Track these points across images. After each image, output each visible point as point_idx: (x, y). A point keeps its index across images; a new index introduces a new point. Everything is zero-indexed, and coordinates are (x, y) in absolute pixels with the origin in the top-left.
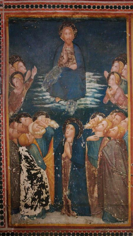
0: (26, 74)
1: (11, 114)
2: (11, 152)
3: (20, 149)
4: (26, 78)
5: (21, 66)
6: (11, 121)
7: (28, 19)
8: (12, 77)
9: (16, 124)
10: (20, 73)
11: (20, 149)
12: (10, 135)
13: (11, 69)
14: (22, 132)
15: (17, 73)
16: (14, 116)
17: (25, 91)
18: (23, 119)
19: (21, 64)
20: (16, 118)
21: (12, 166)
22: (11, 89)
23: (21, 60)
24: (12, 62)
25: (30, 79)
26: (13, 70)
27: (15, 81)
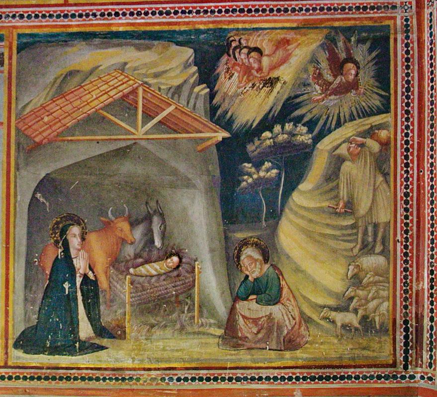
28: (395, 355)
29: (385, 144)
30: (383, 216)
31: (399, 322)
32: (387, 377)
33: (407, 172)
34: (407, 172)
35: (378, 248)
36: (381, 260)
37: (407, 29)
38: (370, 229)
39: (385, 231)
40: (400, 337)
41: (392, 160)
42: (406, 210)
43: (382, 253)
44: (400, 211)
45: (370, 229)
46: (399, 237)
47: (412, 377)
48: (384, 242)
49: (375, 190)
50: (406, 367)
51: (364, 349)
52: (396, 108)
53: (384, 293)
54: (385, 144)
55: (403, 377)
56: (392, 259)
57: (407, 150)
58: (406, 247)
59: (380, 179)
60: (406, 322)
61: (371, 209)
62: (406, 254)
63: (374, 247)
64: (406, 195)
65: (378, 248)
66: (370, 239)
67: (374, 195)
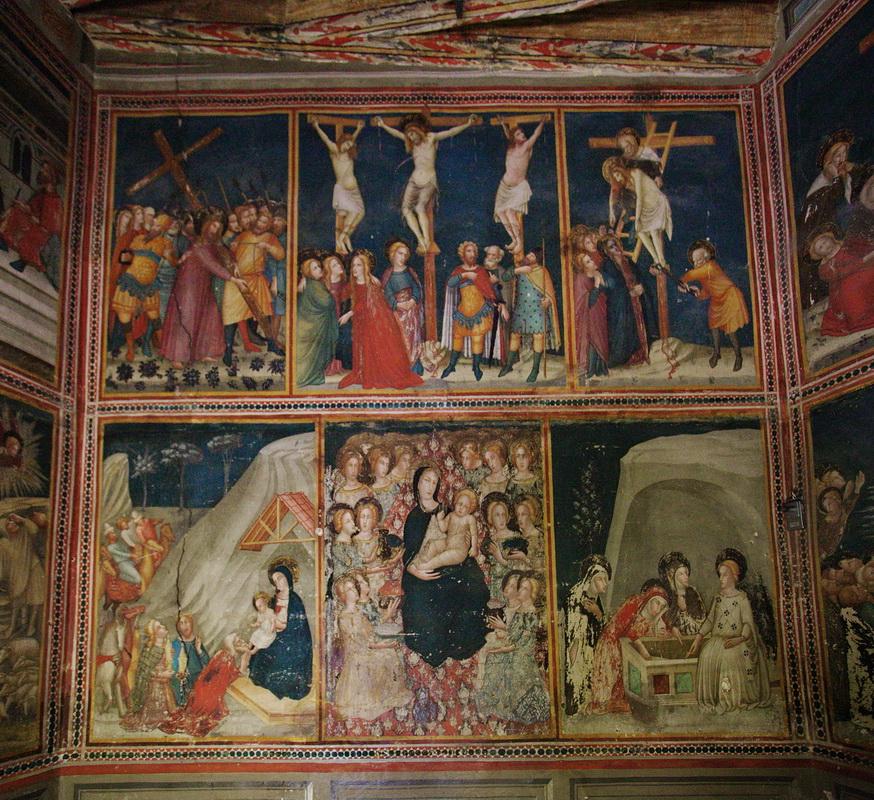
0: (844, 487)
1: (824, 556)
2: (826, 618)
3: (844, 611)
4: (846, 494)
5: (835, 478)
6: (824, 568)
7: (842, 398)
8: (821, 498)
9: (833, 571)
10: (835, 489)
11: (844, 611)
12: (823, 589)
13: (818, 486)
14: (845, 584)
15: (828, 490)
16: (828, 559)
17: (846, 516)
18: (844, 563)
19: (835, 474)
20: (832, 562)
21: (831, 640)
22: (820, 518)
23: (836, 469)
24: (819, 474)
25: (853, 495)
26: (822, 487)
27: (826, 503)
28: (41, 740)
29: (43, 528)
30: (38, 599)
31: (47, 705)
32: (32, 765)
33: (60, 558)
34: (60, 558)
35: (31, 632)
36: (33, 643)
37: (68, 425)
38: (24, 610)
39: (37, 615)
40: (47, 721)
41: (48, 544)
42: (58, 594)
43: (34, 636)
44: (53, 595)
45: (24, 610)
46: (51, 621)
47: (56, 759)
48: (37, 625)
49: (31, 571)
50: (50, 750)
51: (10, 740)
52: (54, 495)
53: (34, 677)
54: (43, 528)
55: (47, 761)
56: (43, 641)
57: (62, 537)
58: (56, 630)
59: (36, 561)
60: (53, 705)
61: (26, 590)
62: (56, 637)
63: (26, 630)
64: (59, 579)
65: (31, 632)
66: (23, 621)
67: (30, 576)
